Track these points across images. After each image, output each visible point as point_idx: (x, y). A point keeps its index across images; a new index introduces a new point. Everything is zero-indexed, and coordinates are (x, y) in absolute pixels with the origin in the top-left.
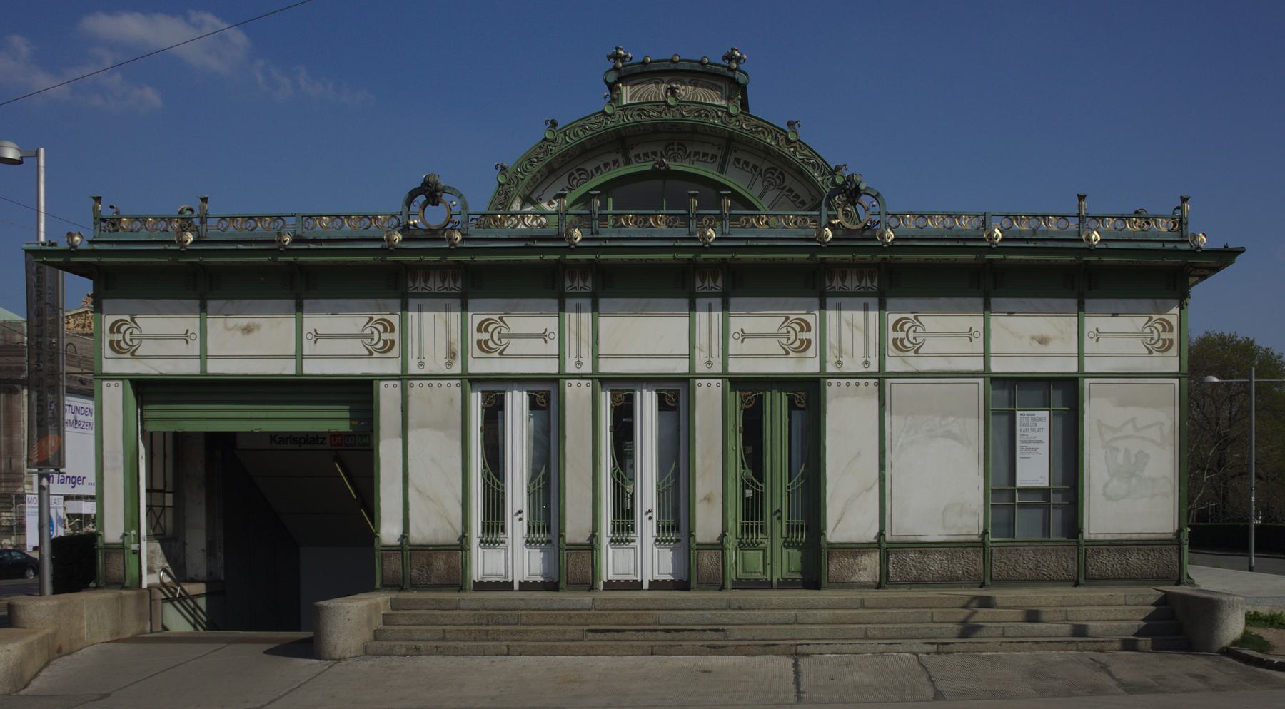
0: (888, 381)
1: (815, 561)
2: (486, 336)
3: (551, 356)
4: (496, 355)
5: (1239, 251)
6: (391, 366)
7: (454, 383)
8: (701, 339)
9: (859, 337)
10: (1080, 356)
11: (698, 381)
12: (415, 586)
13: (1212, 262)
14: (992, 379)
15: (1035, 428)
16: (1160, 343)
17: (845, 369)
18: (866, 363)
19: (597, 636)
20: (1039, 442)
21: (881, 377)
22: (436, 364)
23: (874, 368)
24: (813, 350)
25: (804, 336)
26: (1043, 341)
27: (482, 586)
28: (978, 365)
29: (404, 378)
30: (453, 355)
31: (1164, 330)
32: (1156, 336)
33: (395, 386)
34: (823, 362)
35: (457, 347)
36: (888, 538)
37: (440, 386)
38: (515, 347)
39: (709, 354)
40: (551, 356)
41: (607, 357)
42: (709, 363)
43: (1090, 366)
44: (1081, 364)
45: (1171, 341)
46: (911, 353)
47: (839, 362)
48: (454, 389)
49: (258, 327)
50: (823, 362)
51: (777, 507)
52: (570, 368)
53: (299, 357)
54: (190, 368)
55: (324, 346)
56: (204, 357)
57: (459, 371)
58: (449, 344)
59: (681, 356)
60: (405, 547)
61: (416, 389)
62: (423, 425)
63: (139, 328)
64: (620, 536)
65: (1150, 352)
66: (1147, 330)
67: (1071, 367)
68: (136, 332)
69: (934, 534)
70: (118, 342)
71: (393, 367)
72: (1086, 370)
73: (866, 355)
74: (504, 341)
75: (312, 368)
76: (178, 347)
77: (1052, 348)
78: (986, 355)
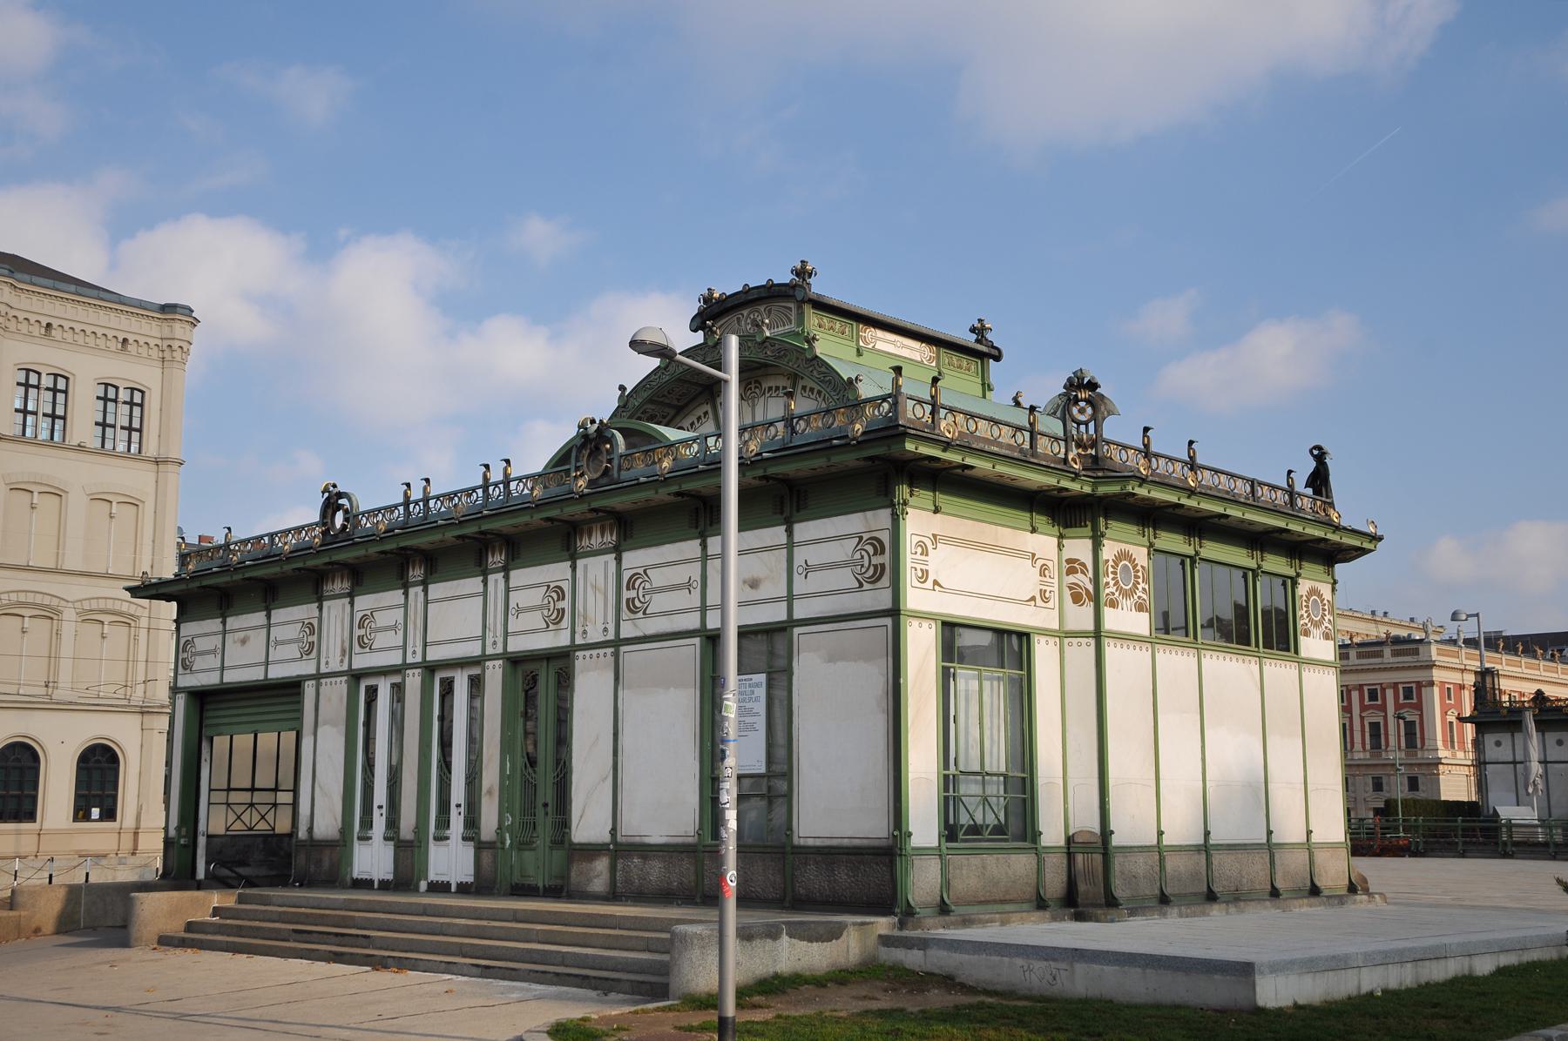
0: (623, 649)
8: (490, 620)
9: (600, 597)
14: (708, 638)
15: (741, 700)
18: (605, 630)
23: (611, 636)
25: (560, 605)
29: (318, 677)
35: (347, 645)
45: (883, 566)
47: (585, 632)
59: (475, 639)
65: (861, 585)
66: (857, 556)
69: (656, 837)
71: (309, 668)
75: (231, 677)
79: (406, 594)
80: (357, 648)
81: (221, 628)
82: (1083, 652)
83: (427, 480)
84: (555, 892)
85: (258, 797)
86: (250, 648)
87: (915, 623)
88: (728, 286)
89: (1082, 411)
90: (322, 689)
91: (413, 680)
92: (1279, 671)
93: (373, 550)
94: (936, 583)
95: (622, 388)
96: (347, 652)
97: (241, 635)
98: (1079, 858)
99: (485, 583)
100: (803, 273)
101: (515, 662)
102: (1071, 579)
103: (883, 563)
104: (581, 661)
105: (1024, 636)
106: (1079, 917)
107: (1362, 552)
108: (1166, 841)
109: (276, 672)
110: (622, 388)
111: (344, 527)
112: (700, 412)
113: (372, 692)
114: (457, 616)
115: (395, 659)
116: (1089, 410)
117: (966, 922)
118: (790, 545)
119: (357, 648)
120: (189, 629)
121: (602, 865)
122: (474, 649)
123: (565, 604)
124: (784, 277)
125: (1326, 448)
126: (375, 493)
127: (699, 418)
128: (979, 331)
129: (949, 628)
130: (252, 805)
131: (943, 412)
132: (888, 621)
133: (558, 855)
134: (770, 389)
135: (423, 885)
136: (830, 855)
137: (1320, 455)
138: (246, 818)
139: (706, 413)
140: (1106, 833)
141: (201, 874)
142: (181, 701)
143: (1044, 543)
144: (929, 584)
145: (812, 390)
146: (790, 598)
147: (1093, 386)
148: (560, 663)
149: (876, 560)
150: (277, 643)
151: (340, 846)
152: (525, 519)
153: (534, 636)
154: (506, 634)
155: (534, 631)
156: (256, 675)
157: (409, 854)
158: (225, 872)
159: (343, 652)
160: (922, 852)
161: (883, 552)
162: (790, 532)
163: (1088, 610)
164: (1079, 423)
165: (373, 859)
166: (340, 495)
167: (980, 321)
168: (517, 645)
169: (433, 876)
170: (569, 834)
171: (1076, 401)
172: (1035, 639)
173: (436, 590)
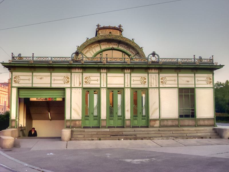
0: (160, 89)
1: (148, 123)
2: (86, 80)
4: (88, 84)
5: (224, 65)
7: (157, 89)
8: (126, 81)
9: (155, 81)
10: (195, 84)
11: (125, 89)
12: (73, 127)
13: (219, 67)
16: (209, 82)
17: (153, 87)
19: (113, 136)
21: (159, 88)
22: (77, 86)
23: (158, 86)
25: (145, 80)
26: (188, 82)
28: (176, 86)
29: (71, 88)
30: (80, 84)
32: (208, 81)
33: (69, 89)
34: (148, 85)
35: (81, 82)
36: (161, 118)
37: (78, 89)
38: (92, 82)
39: (128, 84)
41: (109, 84)
42: (128, 85)
43: (197, 86)
44: (195, 86)
45: (211, 82)
46: (164, 84)
49: (43, 78)
50: (148, 85)
51: (140, 112)
52: (102, 86)
53: (51, 84)
54: (30, 86)
55: (56, 82)
56: (32, 83)
57: (81, 87)
58: (80, 82)
59: (122, 84)
60: (71, 121)
61: (73, 90)
63: (20, 78)
64: (111, 118)
67: (193, 86)
68: (19, 79)
70: (16, 80)
71: (69, 86)
72: (196, 87)
73: (156, 84)
74: (90, 81)
76: (27, 82)
77: (190, 83)
78: (178, 84)
79: (100, 74)
90: (72, 90)
99: (124, 75)
100: (120, 26)
119: (84, 83)
124: (117, 26)
127: (96, 46)
136: (204, 119)
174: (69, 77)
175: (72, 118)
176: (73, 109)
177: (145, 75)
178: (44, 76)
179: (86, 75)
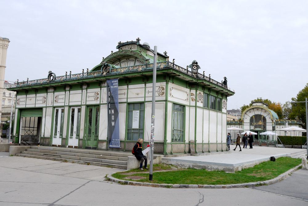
3: (63, 102)
6: (44, 105)
8: (83, 98)
14: (128, 103)
20: (137, 118)
24: (99, 99)
25: (98, 96)
26: (138, 94)
27: (53, 146)
28: (126, 101)
29: (46, 107)
31: (162, 90)
35: (53, 101)
38: (60, 101)
40: (63, 102)
45: (164, 92)
47: (103, 101)
48: (51, 109)
58: (52, 101)
59: (80, 101)
62: (47, 116)
65: (159, 95)
66: (159, 90)
71: (45, 106)
75: (28, 106)
79: (65, 93)
80: (54, 102)
81: (35, 96)
82: (193, 110)
83: (71, 72)
84: (95, 148)
85: (31, 129)
86: (31, 101)
87: (169, 103)
88: (124, 41)
89: (195, 67)
91: (66, 109)
92: (219, 114)
93: (60, 84)
94: (172, 96)
95: (103, 58)
96: (53, 103)
97: (30, 98)
98: (191, 145)
101: (88, 106)
102: (192, 97)
103: (164, 92)
104: (102, 107)
105: (184, 106)
106: (191, 155)
107: (231, 95)
108: (210, 142)
109: (37, 106)
110: (103, 58)
111: (53, 79)
112: (117, 63)
113: (57, 111)
114: (76, 97)
115: (63, 104)
116: (196, 67)
117: (176, 156)
118: (145, 87)
119: (54, 102)
120: (19, 97)
121: (105, 144)
122: (79, 103)
123: (99, 96)
125: (227, 77)
126: (60, 73)
128: (165, 53)
129: (175, 104)
130: (29, 130)
131: (175, 65)
132: (165, 102)
133: (96, 142)
134: (131, 60)
135: (67, 146)
137: (225, 79)
138: (28, 132)
139: (118, 64)
140: (195, 141)
141: (20, 142)
142: (17, 110)
143: (188, 90)
144: (171, 96)
145: (139, 61)
146: (145, 97)
147: (197, 63)
148: (97, 107)
149: (162, 91)
150: (38, 100)
151: (50, 138)
152: (74, 82)
153: (92, 101)
154: (86, 101)
155: (92, 101)
156: (33, 106)
157: (65, 140)
158: (24, 142)
159: (52, 103)
160: (168, 143)
161: (164, 90)
162: (145, 85)
163: (194, 102)
164: (194, 70)
165: (57, 141)
166: (52, 73)
167: (165, 51)
168: (88, 103)
169: (69, 145)
170: (98, 138)
171: (194, 65)
172: (186, 107)
173: (72, 92)
174: (46, 97)
175: (45, 136)
176: (46, 127)
177: (98, 90)
178: (32, 97)
179: (56, 94)
